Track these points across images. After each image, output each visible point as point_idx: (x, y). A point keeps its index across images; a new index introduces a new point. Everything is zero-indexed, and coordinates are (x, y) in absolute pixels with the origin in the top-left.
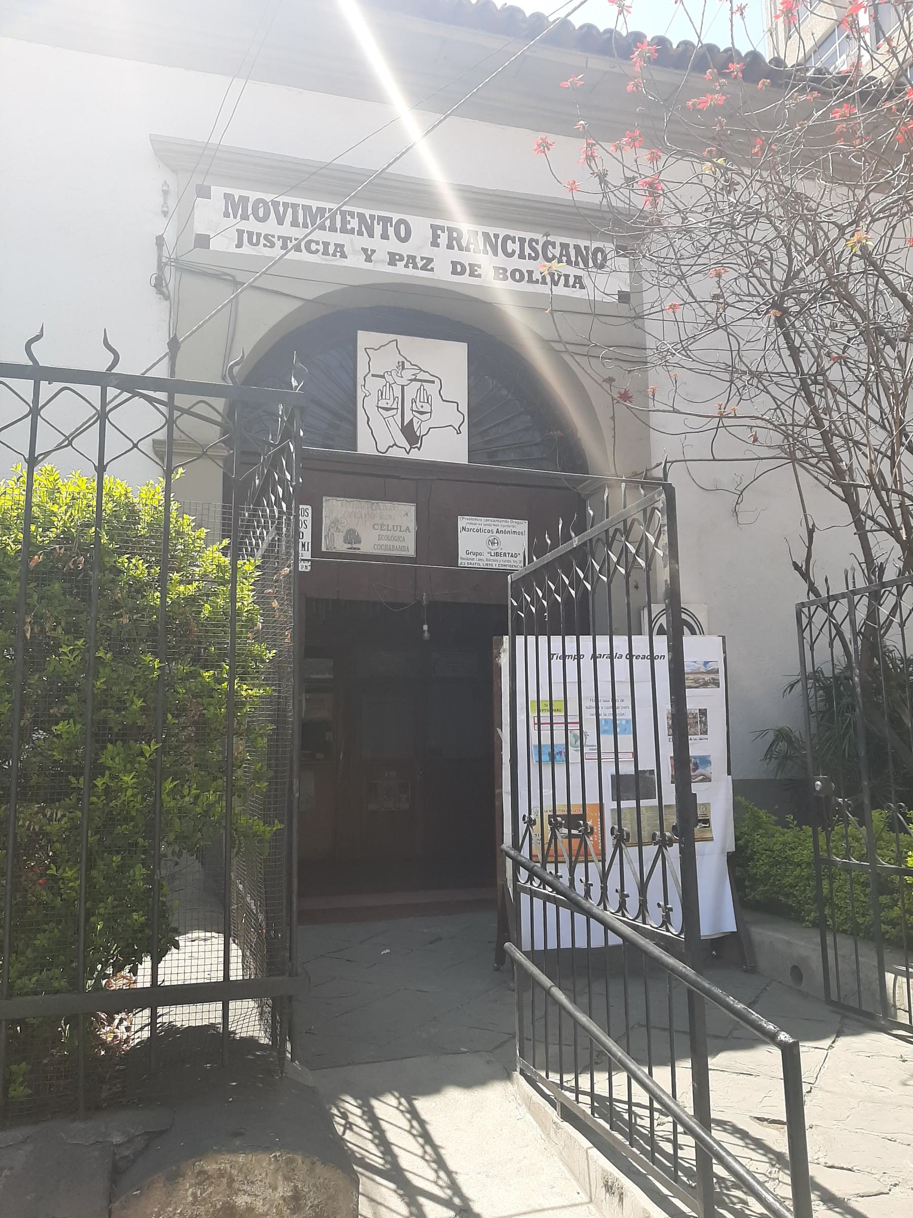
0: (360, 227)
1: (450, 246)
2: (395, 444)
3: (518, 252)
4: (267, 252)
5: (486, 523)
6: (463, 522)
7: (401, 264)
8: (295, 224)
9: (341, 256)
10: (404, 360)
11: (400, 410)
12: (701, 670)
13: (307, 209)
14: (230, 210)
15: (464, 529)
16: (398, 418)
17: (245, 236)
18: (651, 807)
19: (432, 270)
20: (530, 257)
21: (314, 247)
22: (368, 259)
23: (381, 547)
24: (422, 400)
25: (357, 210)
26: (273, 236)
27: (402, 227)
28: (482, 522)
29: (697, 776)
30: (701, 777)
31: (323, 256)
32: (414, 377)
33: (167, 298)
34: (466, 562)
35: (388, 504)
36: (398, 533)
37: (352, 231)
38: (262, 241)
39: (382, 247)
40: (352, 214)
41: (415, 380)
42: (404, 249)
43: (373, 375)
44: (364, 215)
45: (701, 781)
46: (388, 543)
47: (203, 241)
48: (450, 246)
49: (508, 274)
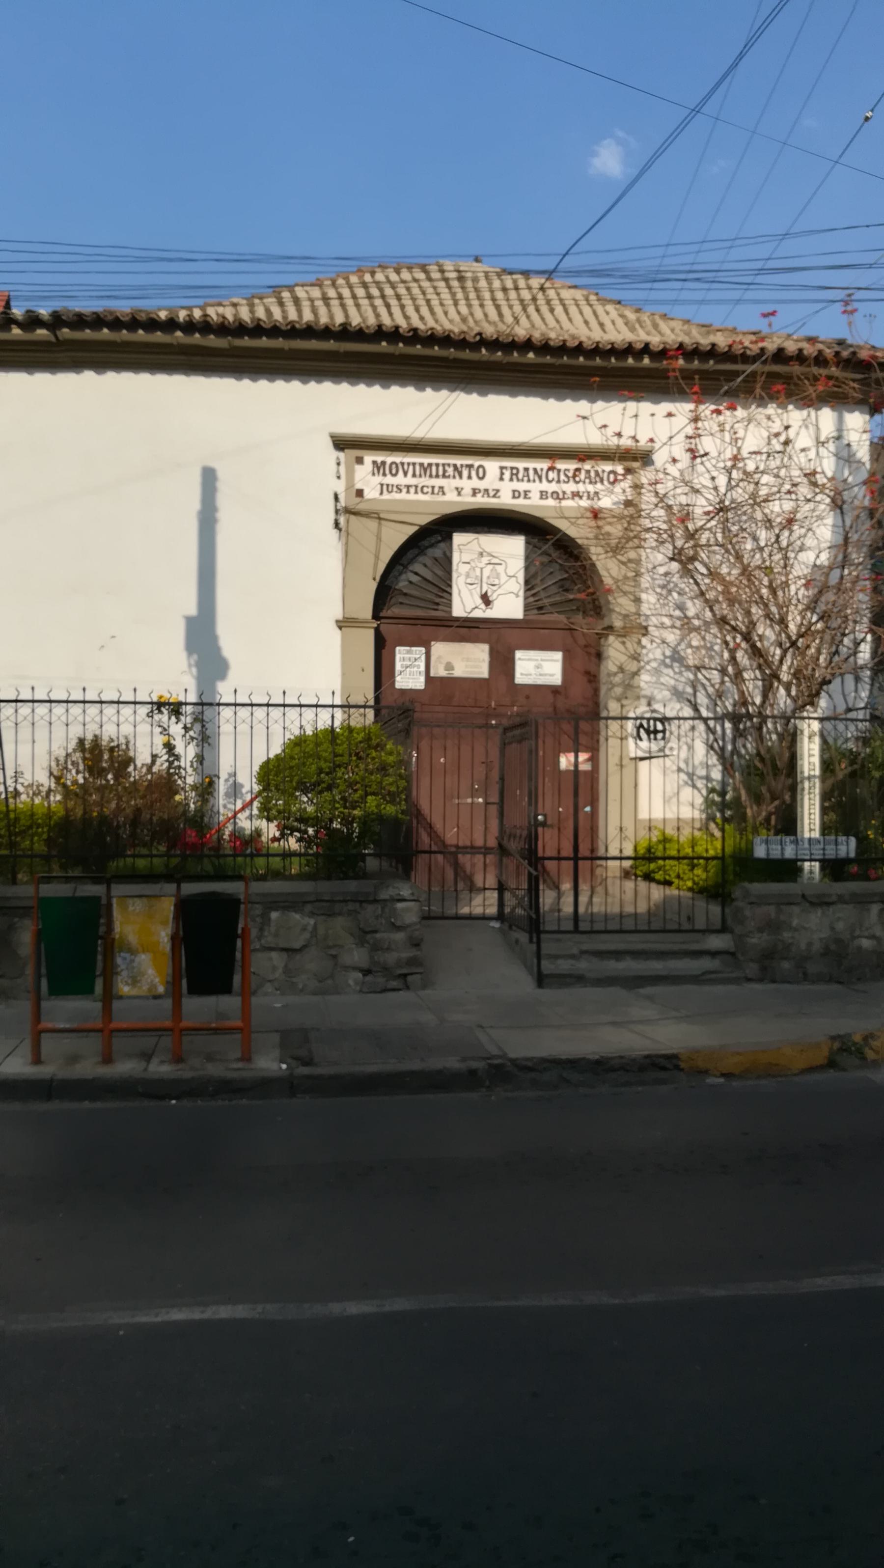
3: (556, 479)
6: (519, 654)
7: (479, 496)
13: (421, 465)
15: (520, 659)
16: (478, 589)
17: (385, 487)
19: (499, 497)
20: (564, 482)
21: (425, 490)
22: (459, 494)
27: (481, 470)
37: (449, 477)
39: (467, 485)
40: (449, 465)
42: (481, 485)
47: (360, 493)
48: (511, 480)
49: (549, 495)
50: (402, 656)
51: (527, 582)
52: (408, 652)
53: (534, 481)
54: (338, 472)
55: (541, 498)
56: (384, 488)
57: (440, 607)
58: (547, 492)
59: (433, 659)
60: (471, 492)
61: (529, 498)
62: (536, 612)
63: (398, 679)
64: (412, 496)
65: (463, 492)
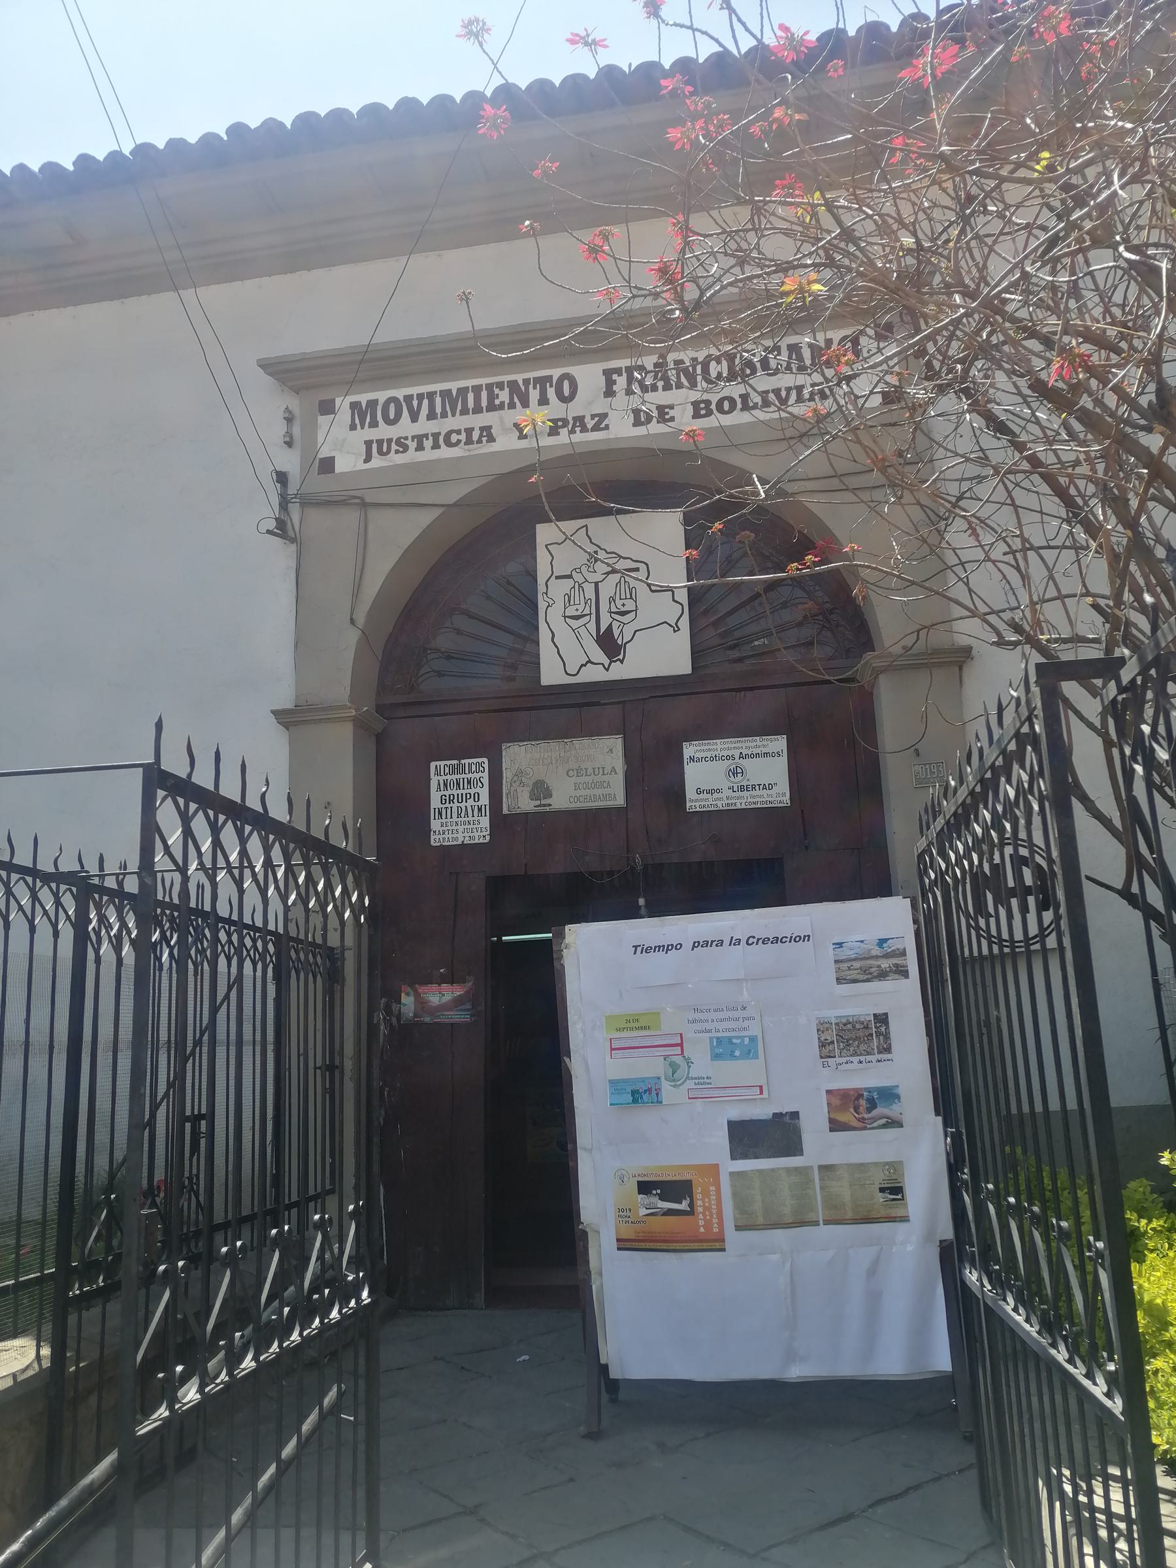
0: (511, 398)
2: (589, 661)
4: (400, 459)
5: (723, 746)
6: (689, 750)
7: (564, 432)
8: (432, 416)
9: (488, 441)
11: (593, 616)
12: (874, 953)
13: (446, 394)
14: (357, 421)
15: (692, 759)
16: (592, 627)
17: (375, 446)
18: (796, 1169)
19: (607, 427)
23: (579, 799)
25: (506, 378)
26: (406, 438)
27: (566, 384)
28: (720, 746)
29: (874, 1119)
30: (883, 1121)
31: (467, 447)
33: (293, 540)
34: (697, 804)
35: (586, 741)
36: (600, 778)
37: (501, 407)
38: (394, 447)
40: (500, 385)
43: (557, 578)
44: (516, 381)
45: (885, 1126)
46: (588, 792)
47: (327, 465)
48: (629, 392)
49: (713, 407)
50: (441, 779)
52: (454, 770)
53: (679, 386)
54: (289, 434)
55: (696, 415)
58: (708, 403)
59: (507, 775)
61: (672, 419)
63: (435, 824)
64: (428, 455)
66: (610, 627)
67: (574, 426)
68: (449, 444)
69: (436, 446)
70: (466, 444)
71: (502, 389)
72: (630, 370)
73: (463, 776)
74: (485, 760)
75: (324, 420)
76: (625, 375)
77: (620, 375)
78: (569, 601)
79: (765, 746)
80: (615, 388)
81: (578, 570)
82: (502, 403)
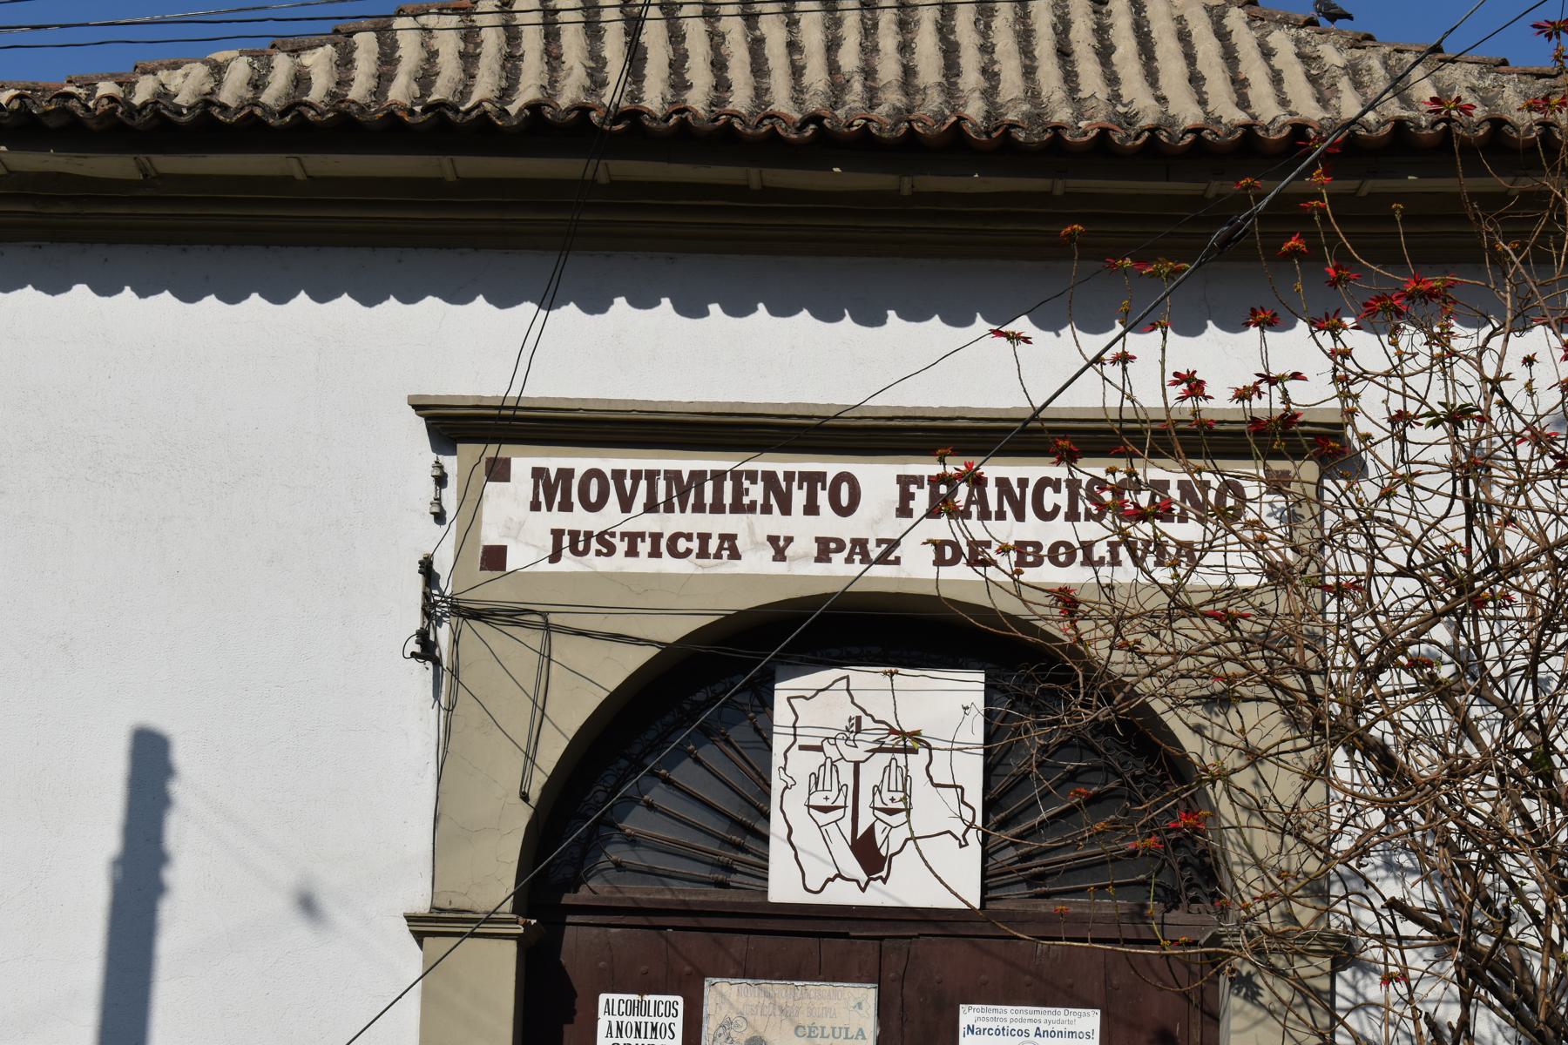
0: (767, 498)
1: (933, 513)
3: (1064, 509)
5: (1014, 1016)
7: (838, 558)
8: (651, 507)
10: (861, 714)
13: (673, 476)
14: (542, 498)
15: (970, 1029)
17: (566, 540)
19: (897, 561)
21: (682, 545)
22: (780, 555)
24: (893, 787)
27: (845, 488)
31: (700, 561)
32: (877, 746)
35: (825, 988)
37: (751, 508)
38: (594, 545)
39: (802, 529)
40: (752, 476)
41: (881, 750)
42: (846, 528)
43: (802, 748)
47: (495, 558)
48: (933, 513)
50: (614, 1019)
51: (989, 806)
52: (634, 1009)
53: (1001, 515)
56: (563, 543)
57: (735, 879)
58: (1038, 546)
60: (814, 549)
62: (1023, 889)
65: (788, 552)
66: (871, 829)
67: (852, 552)
68: (675, 553)
69: (655, 553)
70: (699, 556)
71: (754, 482)
72: (935, 481)
73: (646, 1019)
74: (680, 999)
75: (492, 487)
76: (927, 487)
77: (921, 487)
78: (817, 784)
79: (1070, 1022)
80: (912, 504)
81: (832, 741)
82: (753, 503)
